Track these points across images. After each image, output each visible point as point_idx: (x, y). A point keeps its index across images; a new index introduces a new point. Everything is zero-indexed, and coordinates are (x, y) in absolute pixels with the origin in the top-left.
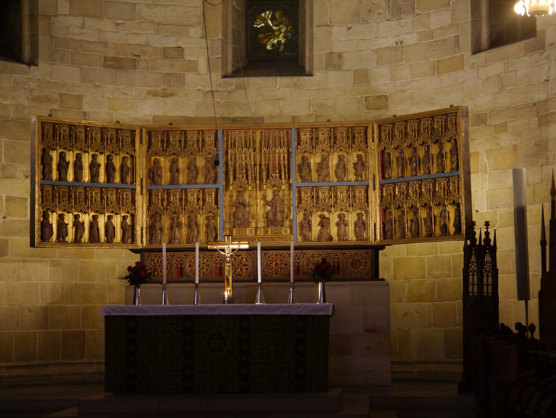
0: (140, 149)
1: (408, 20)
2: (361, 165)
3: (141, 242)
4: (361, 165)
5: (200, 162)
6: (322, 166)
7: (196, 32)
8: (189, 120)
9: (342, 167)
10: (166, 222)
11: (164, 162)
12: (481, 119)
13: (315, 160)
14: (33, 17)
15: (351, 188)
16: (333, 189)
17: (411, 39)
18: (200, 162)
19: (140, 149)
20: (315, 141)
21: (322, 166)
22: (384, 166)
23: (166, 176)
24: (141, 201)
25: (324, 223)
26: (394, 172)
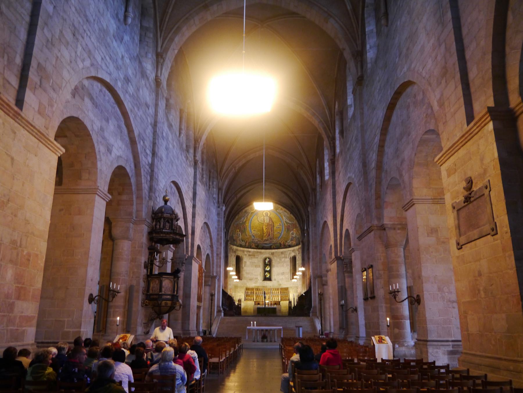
0: (255, 290)
1: (283, 276)
2: (278, 292)
3: (255, 301)
4: (278, 292)
5: (261, 292)
6: (274, 293)
7: (259, 276)
8: (258, 286)
9: (276, 293)
10: (257, 298)
11: (257, 292)
12: (291, 288)
13: (273, 292)
14: (242, 275)
15: (277, 295)
16: (275, 295)
17: (284, 278)
18: (261, 292)
19: (255, 290)
20: (273, 290)
21: (274, 293)
22: (281, 293)
23: (257, 293)
24: (255, 296)
25: (274, 299)
26: (282, 293)
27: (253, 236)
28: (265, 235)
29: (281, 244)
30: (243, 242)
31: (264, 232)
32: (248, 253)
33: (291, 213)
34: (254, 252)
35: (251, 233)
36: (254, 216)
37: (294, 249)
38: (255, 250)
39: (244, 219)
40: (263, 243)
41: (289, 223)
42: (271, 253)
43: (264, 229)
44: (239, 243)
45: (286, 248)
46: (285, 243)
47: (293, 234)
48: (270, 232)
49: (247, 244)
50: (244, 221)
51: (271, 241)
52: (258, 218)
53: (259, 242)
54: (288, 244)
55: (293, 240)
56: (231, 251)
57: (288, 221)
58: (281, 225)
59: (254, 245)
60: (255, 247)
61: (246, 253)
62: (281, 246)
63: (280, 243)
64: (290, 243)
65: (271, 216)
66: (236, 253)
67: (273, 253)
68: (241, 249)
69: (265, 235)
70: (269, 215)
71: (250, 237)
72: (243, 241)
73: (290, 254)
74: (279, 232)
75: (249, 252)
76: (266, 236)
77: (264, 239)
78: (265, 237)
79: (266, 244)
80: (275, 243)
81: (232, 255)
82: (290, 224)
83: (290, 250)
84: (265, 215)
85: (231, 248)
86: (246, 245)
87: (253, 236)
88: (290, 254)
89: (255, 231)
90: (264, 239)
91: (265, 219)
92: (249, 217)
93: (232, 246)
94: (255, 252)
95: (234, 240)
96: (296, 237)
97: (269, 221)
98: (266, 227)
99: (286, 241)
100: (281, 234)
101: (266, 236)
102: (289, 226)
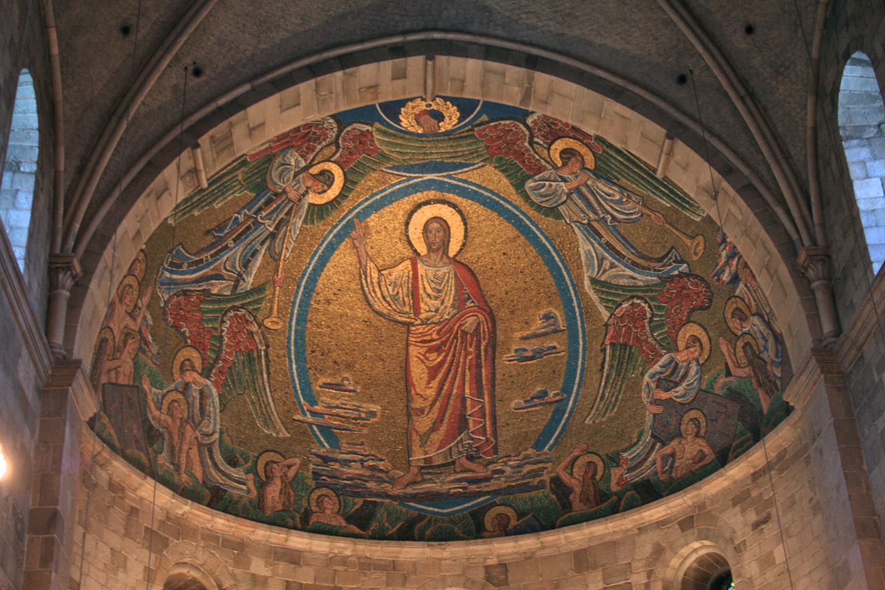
27: (325, 429)
28: (423, 424)
29: (570, 490)
30: (235, 473)
31: (418, 403)
32: (282, 566)
33: (669, 136)
34: (330, 560)
35: (312, 401)
36: (332, 248)
37: (701, 506)
38: (344, 547)
39: (246, 265)
40: (409, 490)
41: (632, 291)
42: (480, 575)
43: (418, 371)
44: (199, 474)
45: (615, 511)
46: (607, 478)
47: (667, 382)
48: (464, 400)
49: (274, 492)
50: (249, 282)
51: (481, 473)
52: (363, 272)
53: (371, 485)
54: (634, 477)
55: (680, 435)
56: (117, 516)
57: (623, 275)
58: (556, 331)
59: (331, 505)
60: (339, 522)
61: (259, 567)
62: (567, 506)
63: (556, 481)
64: (644, 472)
65: (468, 257)
66: (171, 557)
67: (503, 566)
68: (221, 522)
69: (423, 424)
70: (453, 249)
71: (301, 432)
72: (233, 463)
73: (658, 552)
74: (545, 393)
75: (294, 558)
76: (437, 437)
77: (418, 456)
78: (425, 438)
79: (433, 498)
80: (509, 490)
81: (118, 562)
82: (648, 288)
83: (661, 524)
84: (422, 249)
85: (116, 488)
86: (261, 497)
87: (325, 429)
88: (658, 552)
89: (338, 387)
90: (418, 456)
91: (426, 287)
92: (286, 254)
93: (119, 468)
94: (344, 561)
95: (151, 435)
96: (703, 394)
97: (460, 302)
98: (435, 358)
99: (613, 460)
100: (563, 402)
101: (437, 437)
102: (636, 317)
